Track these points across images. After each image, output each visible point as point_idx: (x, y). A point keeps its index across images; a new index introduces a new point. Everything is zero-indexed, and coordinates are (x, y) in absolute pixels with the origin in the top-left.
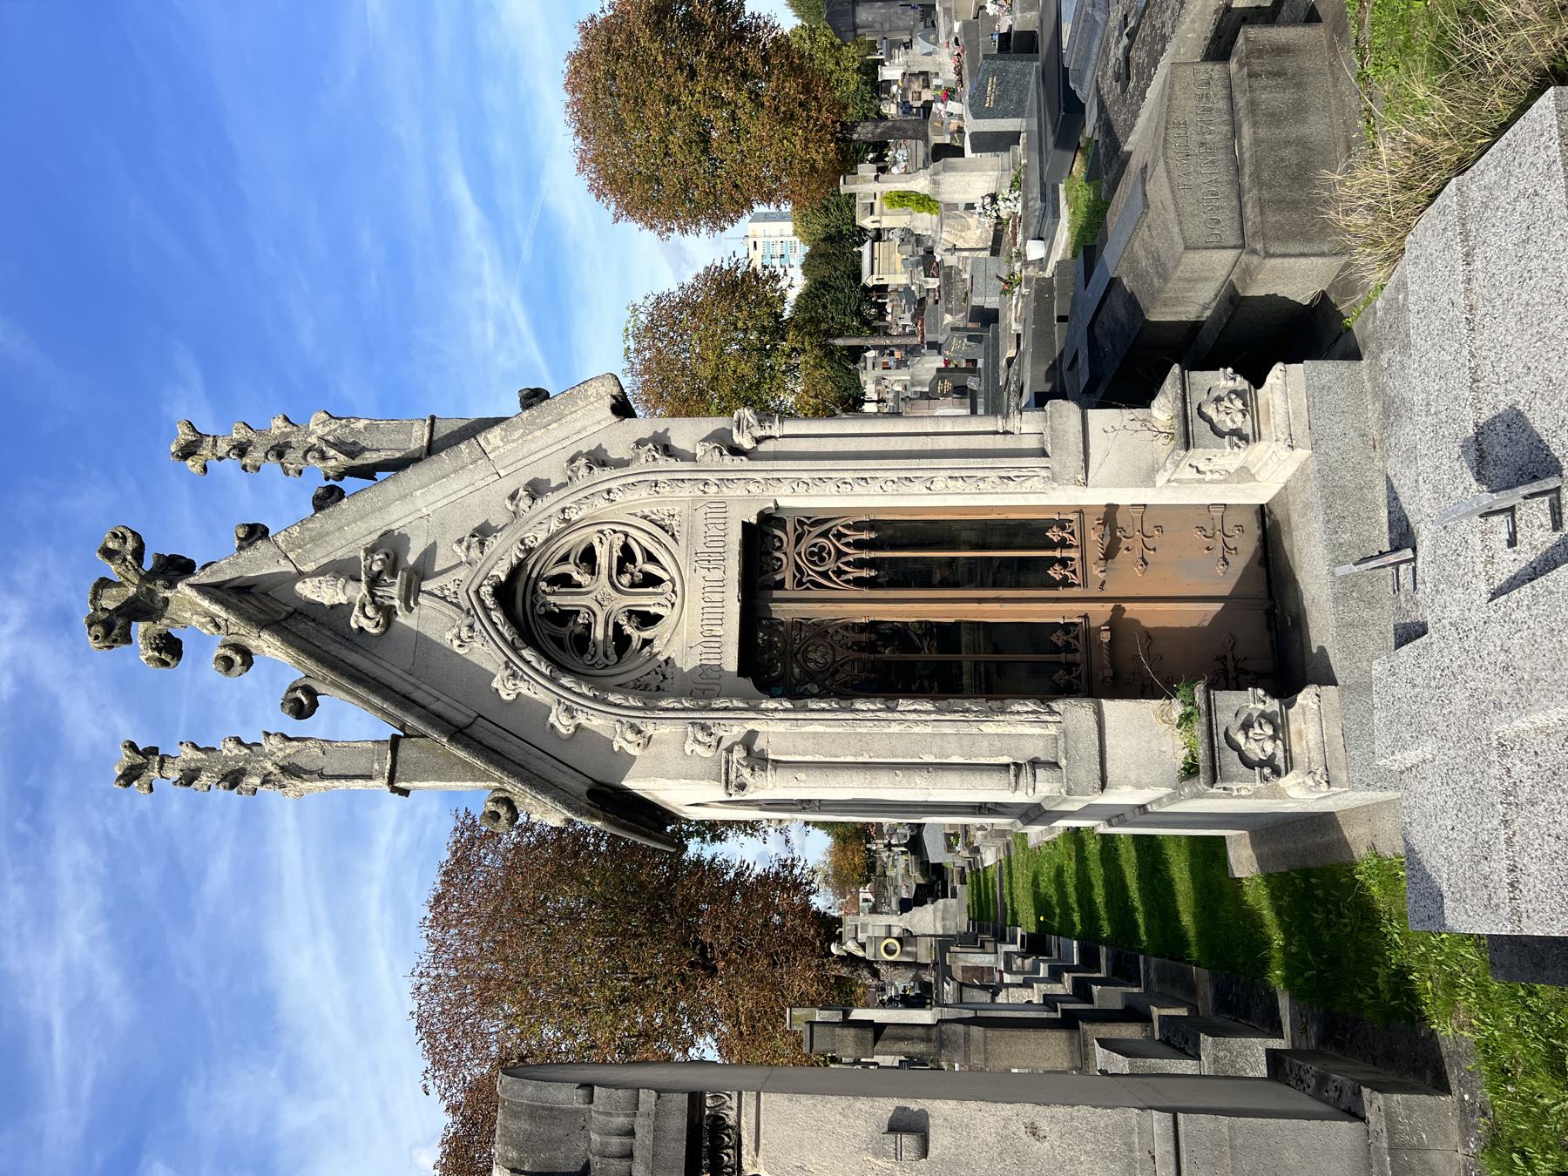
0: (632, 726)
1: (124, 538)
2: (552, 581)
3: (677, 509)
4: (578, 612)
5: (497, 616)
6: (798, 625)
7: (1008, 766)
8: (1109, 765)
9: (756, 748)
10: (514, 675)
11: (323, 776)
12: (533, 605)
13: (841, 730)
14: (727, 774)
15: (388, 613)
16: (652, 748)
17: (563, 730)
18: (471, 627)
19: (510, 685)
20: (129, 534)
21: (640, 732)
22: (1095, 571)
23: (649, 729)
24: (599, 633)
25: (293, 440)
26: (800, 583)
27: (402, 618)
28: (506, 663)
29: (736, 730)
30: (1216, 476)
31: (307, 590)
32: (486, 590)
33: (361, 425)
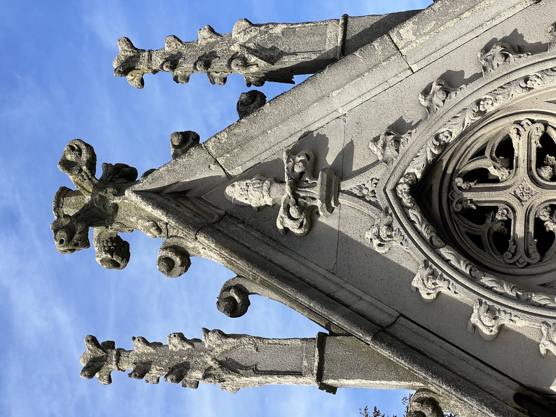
1: (80, 150)
2: (469, 176)
4: (496, 209)
10: (433, 274)
11: (257, 372)
12: (450, 202)
15: (311, 213)
17: (486, 332)
19: (429, 284)
20: (83, 147)
24: (519, 229)
25: (217, 49)
27: (324, 218)
28: (425, 262)
31: (235, 193)
32: (403, 188)
33: (278, 30)
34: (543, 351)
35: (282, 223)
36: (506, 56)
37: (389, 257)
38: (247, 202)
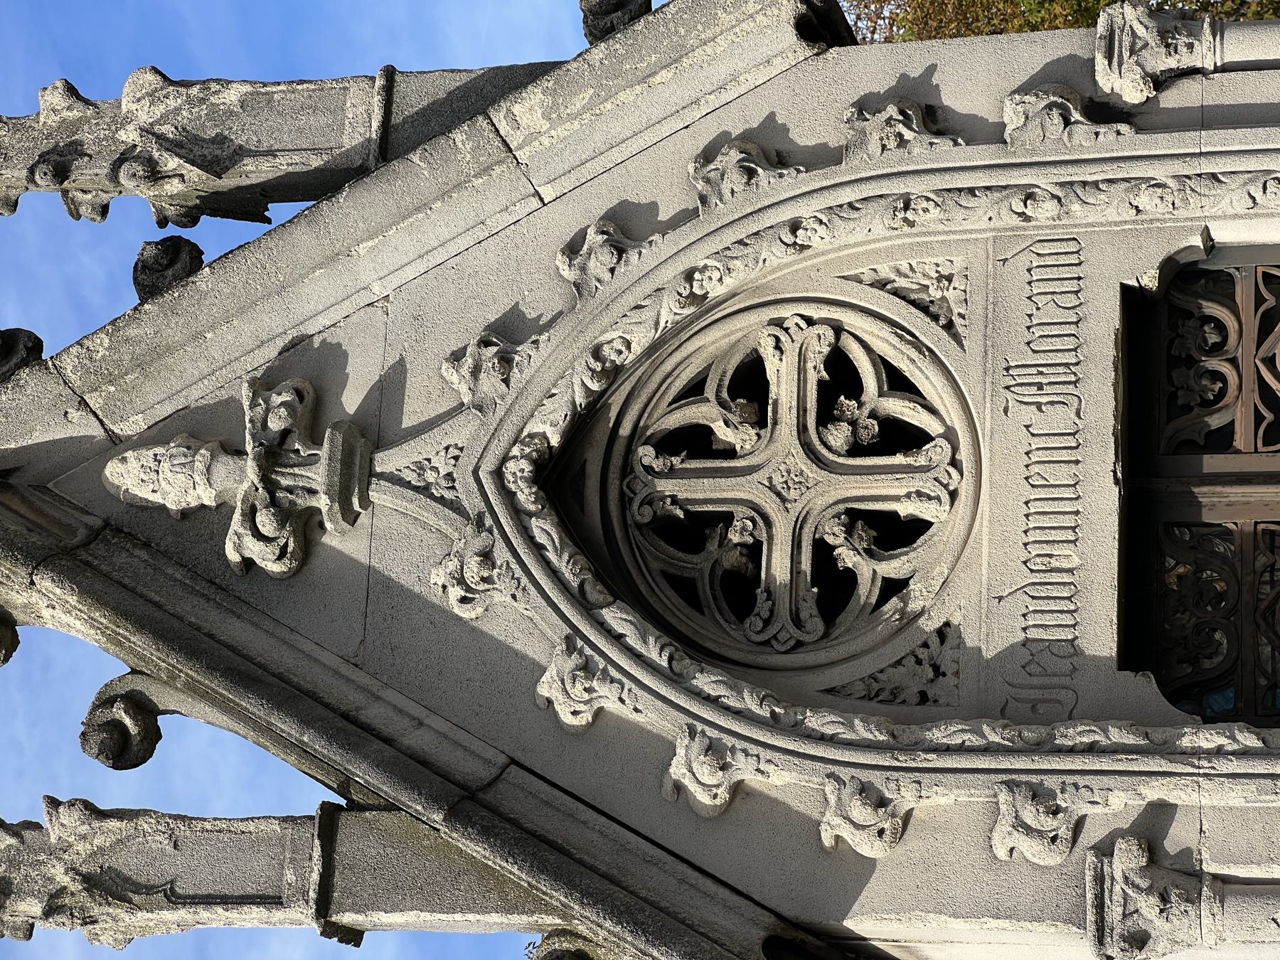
0: (864, 790)
2: (670, 443)
3: (959, 262)
4: (728, 518)
5: (544, 529)
10: (587, 668)
11: (175, 899)
12: (625, 502)
14: (1100, 907)
15: (305, 525)
16: (912, 840)
17: (704, 798)
18: (486, 557)
19: (578, 691)
21: (881, 803)
23: (905, 797)
24: (778, 565)
25: (86, 136)
27: (335, 537)
29: (1118, 800)
31: (128, 476)
32: (519, 468)
33: (231, 96)
34: (827, 841)
35: (238, 548)
36: (751, 173)
37: (486, 627)
38: (157, 498)
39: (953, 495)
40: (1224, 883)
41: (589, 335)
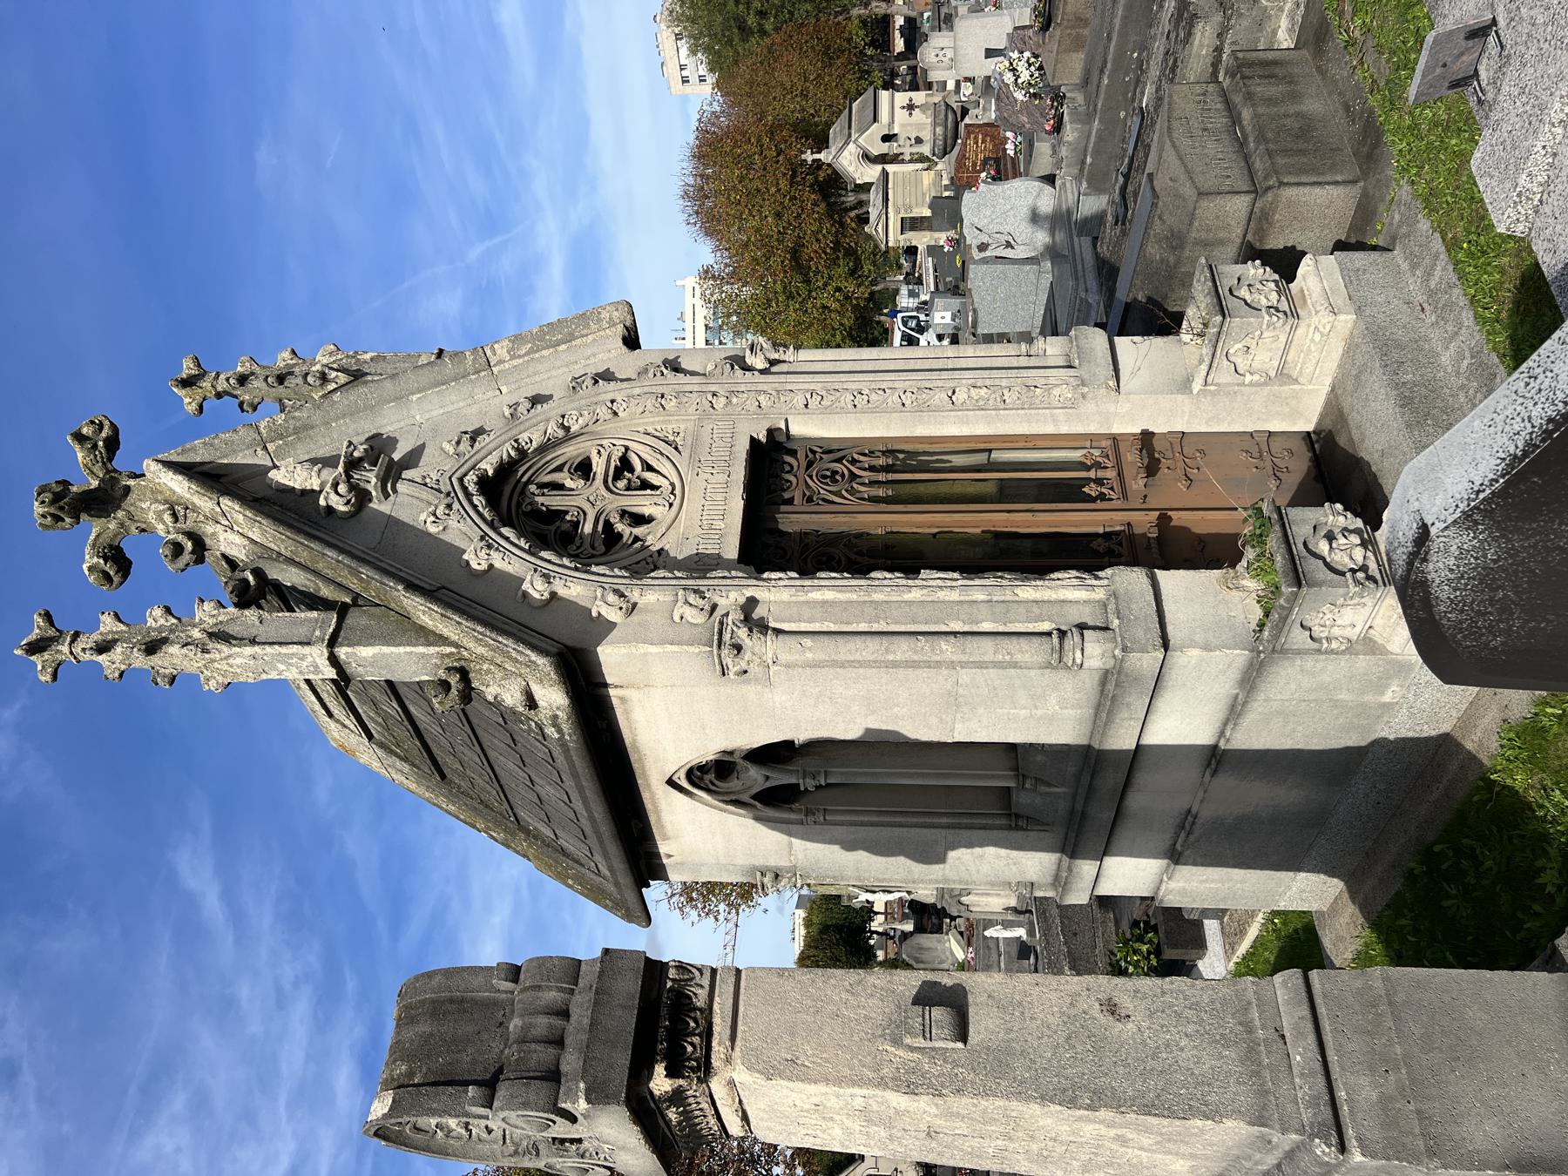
0: (616, 591)
1: (101, 426)
2: (541, 486)
3: (682, 427)
4: (567, 512)
5: (478, 500)
6: (803, 535)
7: (1049, 634)
8: (1170, 629)
9: (755, 616)
10: (489, 547)
11: (253, 642)
12: (519, 505)
13: (854, 597)
14: (720, 634)
15: (362, 497)
16: (635, 617)
17: (537, 596)
18: (449, 506)
19: (482, 554)
20: (106, 423)
21: (622, 595)
22: (1137, 484)
23: (634, 595)
24: (588, 528)
25: (297, 370)
26: (810, 500)
27: (378, 505)
28: (482, 538)
29: (733, 595)
30: (1256, 378)
31: (278, 476)
32: (471, 478)
33: (368, 356)
34: (594, 614)
35: (326, 499)
36: (596, 382)
37: (445, 537)
38: (291, 484)
39: (671, 505)
40: (778, 632)
41: (514, 432)
